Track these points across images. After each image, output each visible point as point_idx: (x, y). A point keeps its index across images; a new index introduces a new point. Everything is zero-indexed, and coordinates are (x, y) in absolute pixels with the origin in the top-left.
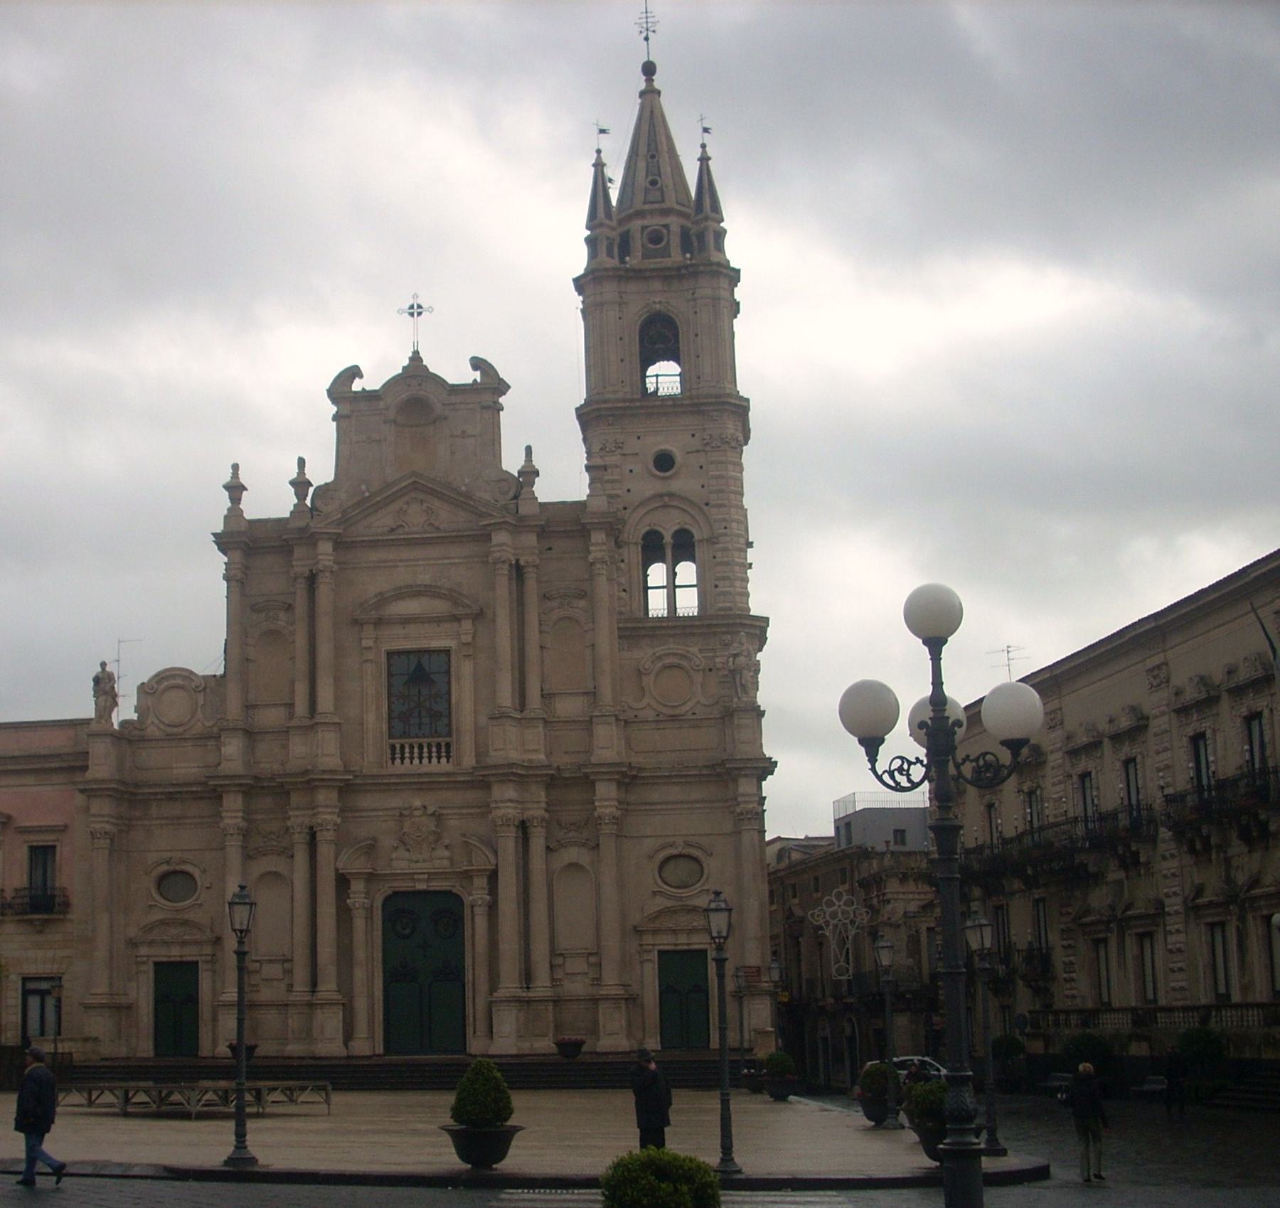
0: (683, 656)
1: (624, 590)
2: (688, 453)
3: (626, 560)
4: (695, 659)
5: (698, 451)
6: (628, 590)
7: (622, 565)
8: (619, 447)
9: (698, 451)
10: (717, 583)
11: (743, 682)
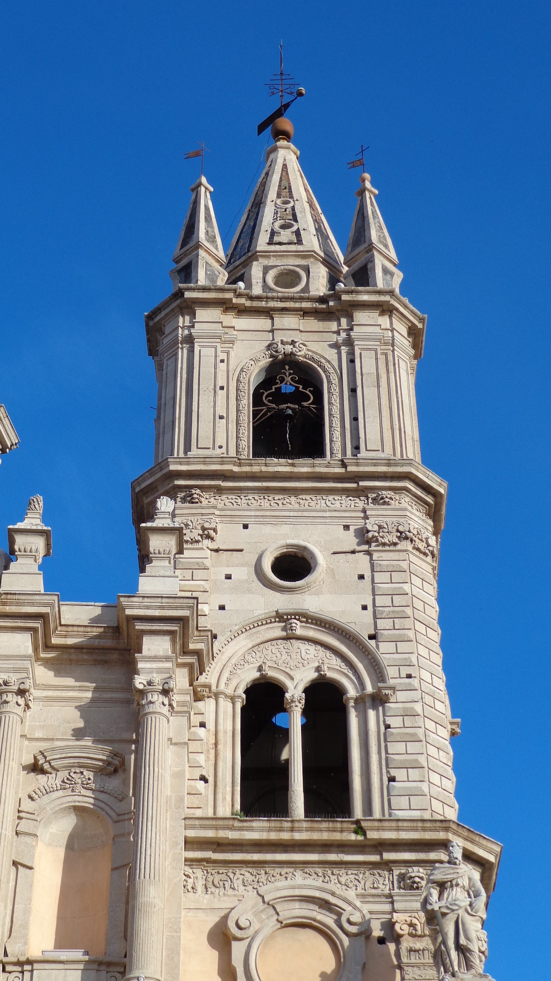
0: (325, 905)
1: (204, 779)
2: (334, 553)
3: (211, 725)
4: (349, 908)
5: (353, 552)
6: (211, 779)
7: (202, 732)
8: (209, 537)
9: (353, 552)
10: (393, 772)
11: (463, 941)
